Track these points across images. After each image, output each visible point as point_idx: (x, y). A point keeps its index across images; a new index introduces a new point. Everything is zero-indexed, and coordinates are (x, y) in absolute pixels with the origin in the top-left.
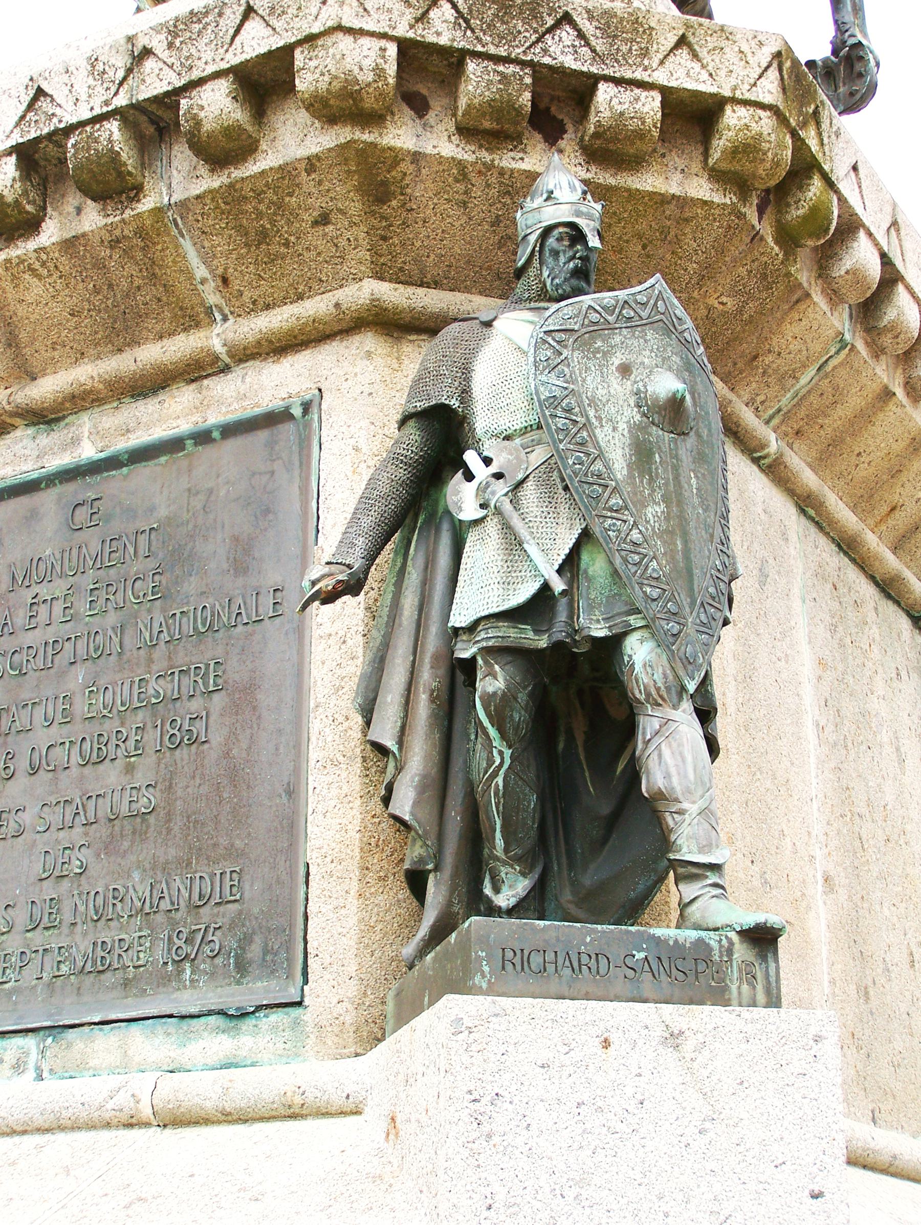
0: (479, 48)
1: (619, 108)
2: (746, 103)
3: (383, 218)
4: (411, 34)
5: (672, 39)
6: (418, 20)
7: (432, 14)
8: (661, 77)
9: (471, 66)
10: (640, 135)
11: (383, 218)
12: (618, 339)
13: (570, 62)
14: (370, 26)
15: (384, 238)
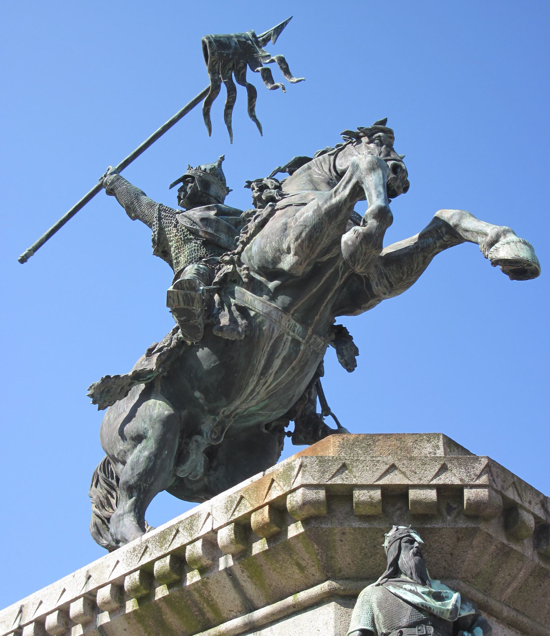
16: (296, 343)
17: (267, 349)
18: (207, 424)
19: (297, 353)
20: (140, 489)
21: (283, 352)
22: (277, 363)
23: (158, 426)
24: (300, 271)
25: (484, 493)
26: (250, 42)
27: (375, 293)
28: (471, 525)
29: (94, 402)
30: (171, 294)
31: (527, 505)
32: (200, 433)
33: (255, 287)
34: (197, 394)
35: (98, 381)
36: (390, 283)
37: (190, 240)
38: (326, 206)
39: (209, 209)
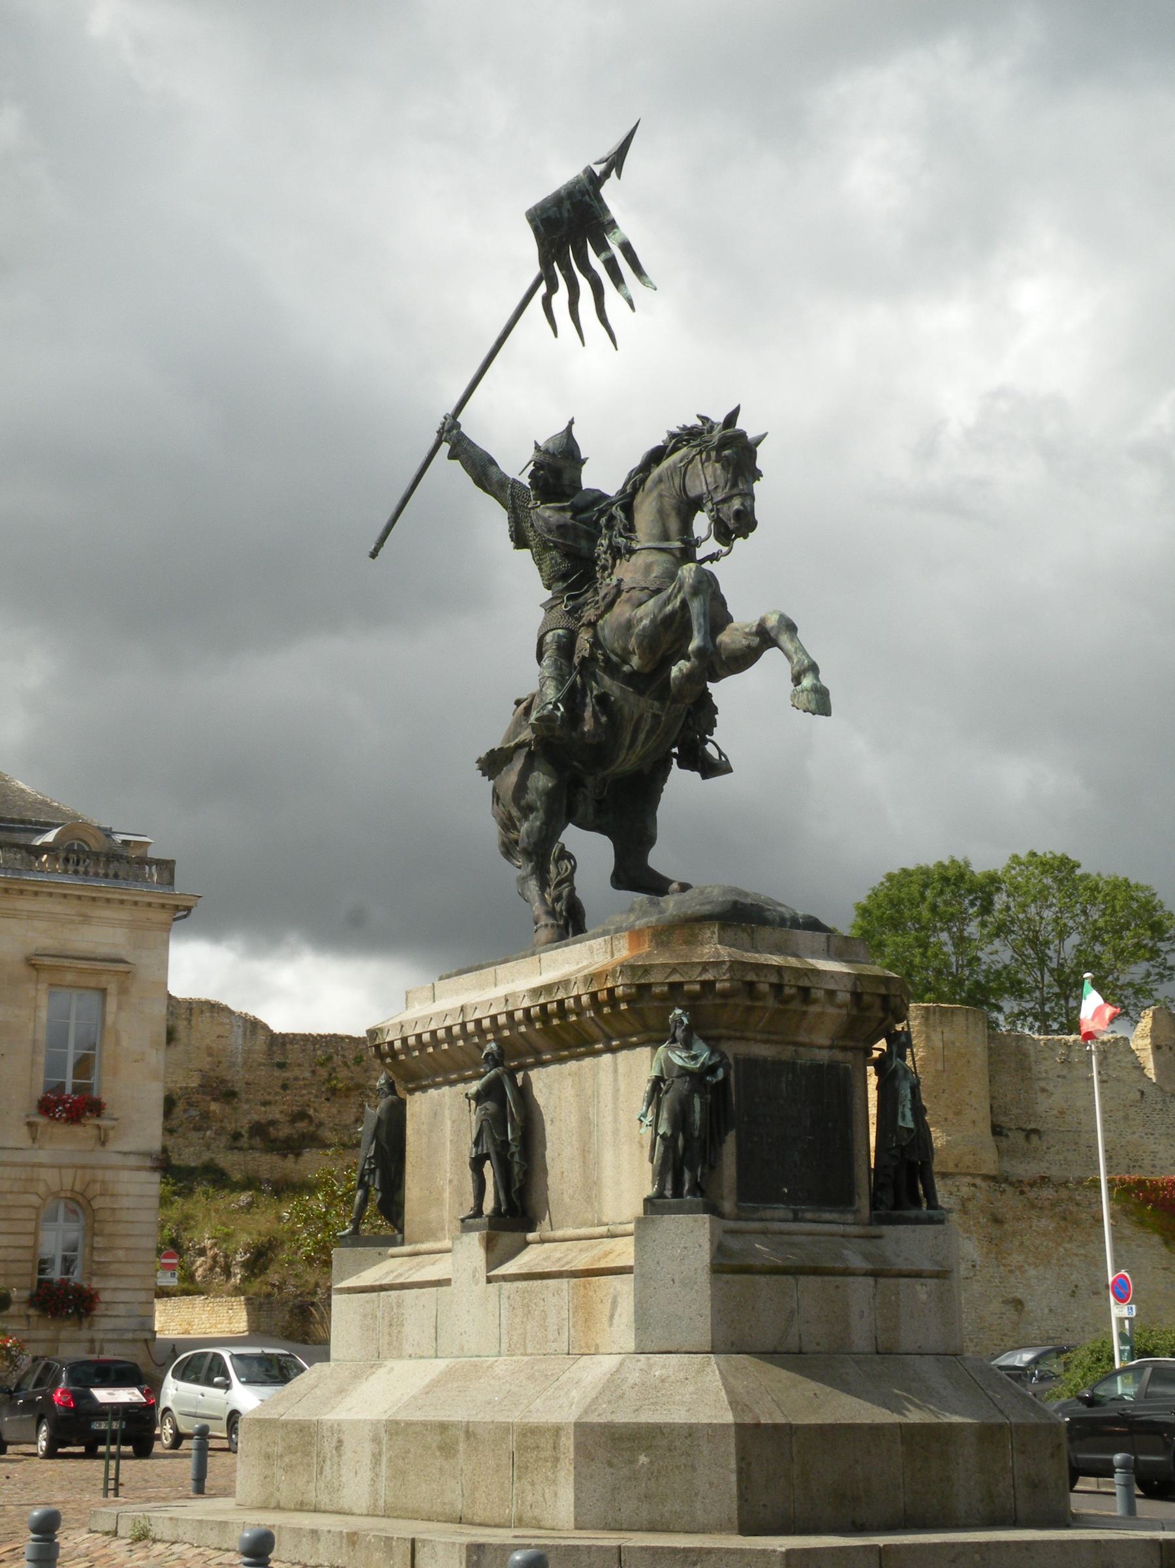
16: (656, 717)
17: (630, 729)
18: (589, 781)
19: (659, 724)
21: (646, 727)
22: (642, 737)
23: (543, 798)
24: (647, 670)
25: (727, 985)
26: (587, 197)
28: (723, 1001)
29: (484, 775)
31: (763, 979)
32: (586, 787)
33: (612, 669)
34: (575, 763)
35: (483, 755)
37: (550, 549)
38: (660, 616)
39: (563, 509)
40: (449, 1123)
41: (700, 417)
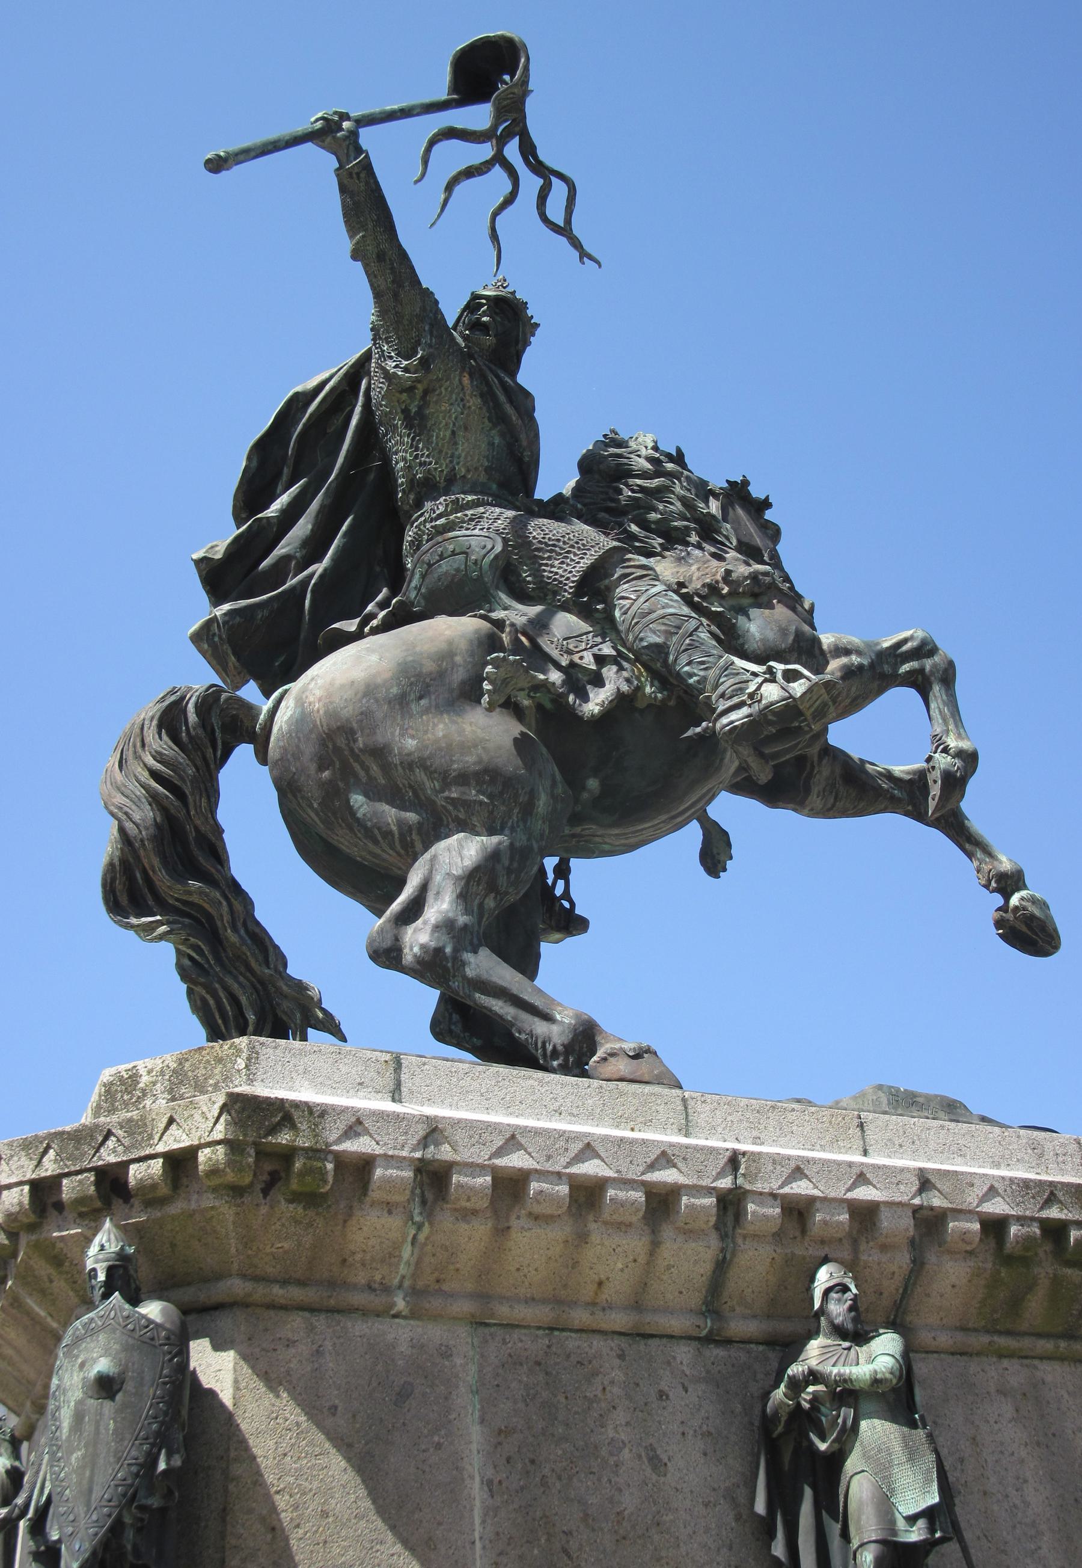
0: (67, 1170)
1: (139, 1176)
2: (209, 1144)
3: (67, 1273)
4: (33, 1176)
5: (165, 1120)
6: (37, 1166)
7: (44, 1160)
8: (161, 1148)
9: (65, 1181)
10: (154, 1186)
11: (67, 1273)
12: (84, 1345)
13: (112, 1159)
14: (13, 1180)
15: (75, 1282)
17: (704, 790)
20: (502, 900)
27: (807, 802)
30: (815, 689)
36: (833, 806)
40: (473, 1440)
41: (679, 450)
